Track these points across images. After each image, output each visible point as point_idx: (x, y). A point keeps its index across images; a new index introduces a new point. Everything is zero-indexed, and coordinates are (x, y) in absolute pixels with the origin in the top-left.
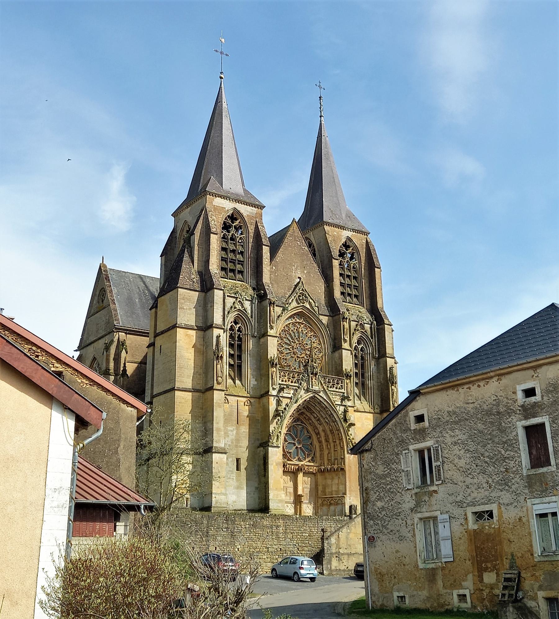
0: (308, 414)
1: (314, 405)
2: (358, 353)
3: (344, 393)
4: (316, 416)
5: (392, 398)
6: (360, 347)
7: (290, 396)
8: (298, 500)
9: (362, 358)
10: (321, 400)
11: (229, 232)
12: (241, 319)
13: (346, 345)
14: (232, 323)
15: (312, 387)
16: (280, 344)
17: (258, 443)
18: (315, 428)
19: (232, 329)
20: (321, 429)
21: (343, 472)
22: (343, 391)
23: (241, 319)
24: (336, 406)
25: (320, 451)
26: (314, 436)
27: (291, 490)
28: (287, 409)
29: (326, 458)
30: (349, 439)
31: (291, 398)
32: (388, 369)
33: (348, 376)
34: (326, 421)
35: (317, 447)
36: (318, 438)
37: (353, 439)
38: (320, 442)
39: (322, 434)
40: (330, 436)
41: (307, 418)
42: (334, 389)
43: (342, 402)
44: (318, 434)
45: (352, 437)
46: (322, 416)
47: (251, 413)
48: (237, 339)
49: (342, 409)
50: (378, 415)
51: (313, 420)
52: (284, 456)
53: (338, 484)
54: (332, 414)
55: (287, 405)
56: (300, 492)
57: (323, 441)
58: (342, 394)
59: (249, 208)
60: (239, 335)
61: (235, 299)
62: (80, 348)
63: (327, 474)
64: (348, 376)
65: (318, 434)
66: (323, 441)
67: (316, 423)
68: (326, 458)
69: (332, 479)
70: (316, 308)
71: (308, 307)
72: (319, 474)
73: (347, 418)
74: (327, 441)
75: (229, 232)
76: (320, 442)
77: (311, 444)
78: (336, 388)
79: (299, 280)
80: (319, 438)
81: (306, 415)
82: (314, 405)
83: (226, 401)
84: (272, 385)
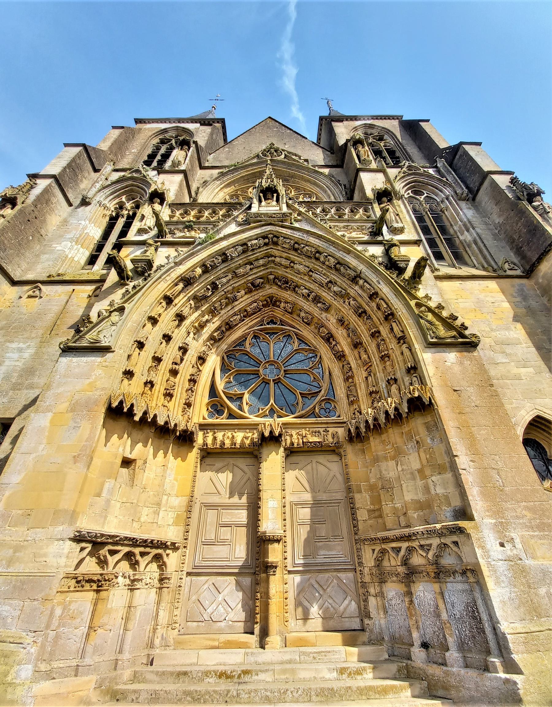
0: (287, 295)
10: (297, 235)
20: (331, 321)
21: (429, 419)
25: (346, 379)
26: (324, 350)
38: (340, 356)
39: (340, 334)
44: (329, 338)
57: (347, 350)
65: (329, 338)
66: (347, 350)
67: (315, 310)
76: (340, 356)
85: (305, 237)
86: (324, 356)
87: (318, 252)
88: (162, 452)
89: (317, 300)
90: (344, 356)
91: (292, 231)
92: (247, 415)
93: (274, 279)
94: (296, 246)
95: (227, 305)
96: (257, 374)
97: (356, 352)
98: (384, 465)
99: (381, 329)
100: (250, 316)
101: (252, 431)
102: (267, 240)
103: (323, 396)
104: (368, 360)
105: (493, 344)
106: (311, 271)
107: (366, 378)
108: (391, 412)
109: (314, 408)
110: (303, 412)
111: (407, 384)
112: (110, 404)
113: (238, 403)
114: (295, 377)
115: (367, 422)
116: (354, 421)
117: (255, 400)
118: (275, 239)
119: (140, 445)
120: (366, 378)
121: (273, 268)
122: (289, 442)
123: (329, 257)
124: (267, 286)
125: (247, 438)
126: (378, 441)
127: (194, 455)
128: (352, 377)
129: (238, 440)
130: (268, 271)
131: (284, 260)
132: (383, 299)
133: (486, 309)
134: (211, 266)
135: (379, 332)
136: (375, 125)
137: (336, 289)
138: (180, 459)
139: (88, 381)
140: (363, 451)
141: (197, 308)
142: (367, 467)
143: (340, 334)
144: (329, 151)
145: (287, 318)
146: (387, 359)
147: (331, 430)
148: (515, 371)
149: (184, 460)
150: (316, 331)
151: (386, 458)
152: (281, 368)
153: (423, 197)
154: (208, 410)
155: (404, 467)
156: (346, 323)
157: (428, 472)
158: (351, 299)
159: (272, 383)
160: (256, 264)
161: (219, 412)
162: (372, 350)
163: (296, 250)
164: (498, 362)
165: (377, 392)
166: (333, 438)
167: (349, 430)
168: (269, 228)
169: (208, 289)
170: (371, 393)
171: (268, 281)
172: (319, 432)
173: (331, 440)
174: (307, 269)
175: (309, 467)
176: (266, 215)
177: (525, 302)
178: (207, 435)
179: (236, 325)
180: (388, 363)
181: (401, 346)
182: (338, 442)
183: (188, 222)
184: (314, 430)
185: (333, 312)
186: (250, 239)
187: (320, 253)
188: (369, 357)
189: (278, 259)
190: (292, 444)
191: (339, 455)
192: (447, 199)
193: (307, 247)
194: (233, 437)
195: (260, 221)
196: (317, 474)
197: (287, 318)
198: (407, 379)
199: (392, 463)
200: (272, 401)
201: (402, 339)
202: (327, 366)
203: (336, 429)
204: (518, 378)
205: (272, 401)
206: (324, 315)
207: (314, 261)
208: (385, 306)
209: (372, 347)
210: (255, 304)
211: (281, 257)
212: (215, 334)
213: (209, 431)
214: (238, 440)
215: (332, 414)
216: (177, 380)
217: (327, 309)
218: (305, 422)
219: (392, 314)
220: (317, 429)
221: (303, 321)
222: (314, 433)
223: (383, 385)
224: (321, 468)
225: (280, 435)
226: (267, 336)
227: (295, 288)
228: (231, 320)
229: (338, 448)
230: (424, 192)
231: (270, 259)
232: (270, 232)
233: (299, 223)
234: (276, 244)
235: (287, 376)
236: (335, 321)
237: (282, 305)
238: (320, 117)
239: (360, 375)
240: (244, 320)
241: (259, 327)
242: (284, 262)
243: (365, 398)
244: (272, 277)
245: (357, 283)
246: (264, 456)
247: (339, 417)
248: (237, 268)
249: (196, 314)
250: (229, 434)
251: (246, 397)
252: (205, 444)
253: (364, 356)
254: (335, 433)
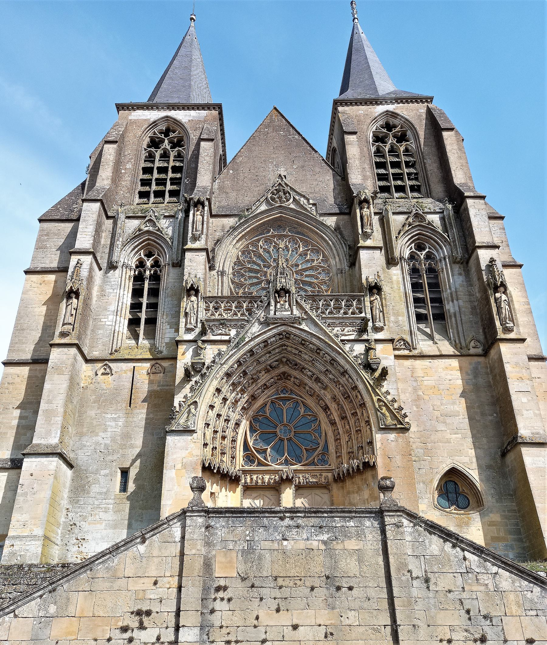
1: (297, 352)
2: (420, 264)
4: (309, 373)
5: (499, 312)
7: (226, 338)
9: (431, 270)
10: (304, 335)
12: (156, 248)
15: (275, 314)
16: (238, 272)
18: (319, 398)
20: (327, 397)
22: (363, 315)
23: (156, 248)
24: (341, 345)
25: (336, 440)
26: (322, 416)
30: (379, 400)
31: (229, 341)
34: (330, 379)
35: (330, 434)
36: (328, 416)
37: (394, 401)
39: (333, 406)
41: (297, 382)
44: (326, 408)
45: (390, 398)
47: (163, 385)
50: (481, 359)
57: (337, 420)
59: (193, 113)
65: (326, 408)
66: (337, 420)
67: (316, 387)
70: (311, 206)
73: (371, 361)
76: (333, 423)
80: (330, 415)
81: (295, 378)
82: (297, 352)
83: (108, 370)
84: (186, 325)
85: (309, 338)
86: (322, 421)
87: (319, 349)
88: (224, 488)
89: (318, 380)
90: (335, 423)
91: (300, 332)
92: (270, 464)
93: (286, 361)
94: (303, 342)
95: (252, 383)
96: (275, 433)
97: (343, 422)
98: (352, 496)
99: (358, 411)
100: (268, 388)
101: (274, 474)
102: (281, 336)
103: (320, 451)
104: (349, 429)
105: (439, 416)
106: (313, 360)
107: (347, 442)
108: (355, 468)
109: (314, 459)
110: (307, 462)
111: (367, 451)
112: (204, 465)
113: (264, 455)
114: (302, 436)
115: (343, 472)
116: (337, 470)
117: (274, 453)
118: (288, 335)
119: (215, 484)
120: (347, 442)
121: (285, 353)
122: (297, 481)
123: (326, 355)
124: (281, 366)
125: (272, 479)
126: (350, 482)
127: (239, 489)
128: (340, 439)
129: (266, 480)
130: (282, 355)
131: (294, 350)
132: (359, 392)
133: (443, 385)
134: (243, 362)
135: (356, 413)
136: (398, 115)
137: (330, 376)
138: (232, 492)
139: (187, 452)
140: (343, 488)
141: (234, 390)
142: (344, 497)
143: (333, 407)
144: (340, 176)
145: (296, 389)
146: (359, 432)
147: (324, 474)
148: (449, 436)
149: (234, 492)
150: (317, 401)
151: (353, 492)
152: (292, 429)
153: (424, 253)
154: (243, 460)
155: (361, 498)
156: (337, 400)
157: (369, 500)
158: (341, 386)
159: (286, 441)
160: (273, 352)
161: (252, 462)
162: (352, 424)
163: (303, 345)
164: (439, 430)
165: (352, 452)
166: (325, 480)
167: (334, 476)
168: (283, 328)
169: (241, 377)
170: (349, 453)
171: (282, 362)
172: (316, 475)
173: (323, 481)
174: (310, 358)
175: (310, 496)
176: (281, 319)
177: (475, 379)
178: (247, 477)
179: (259, 396)
180: (359, 435)
181: (367, 426)
182: (328, 482)
183: (222, 320)
184: (313, 474)
185: (329, 390)
186: (269, 338)
187: (321, 350)
188: (350, 428)
189: (289, 349)
190: (299, 483)
191: (329, 489)
192: (445, 259)
193: (311, 345)
194: (263, 478)
195: (277, 323)
196: (315, 500)
197: (296, 389)
198: (367, 448)
199: (356, 495)
200: (286, 454)
202: (324, 429)
203: (327, 474)
204: (448, 441)
205: (286, 454)
206: (323, 391)
207: (316, 354)
208: (360, 398)
209: (352, 421)
210: (272, 380)
211: (292, 347)
212: (245, 406)
213: (247, 474)
214: (266, 480)
215: (326, 462)
216: (226, 442)
217: (325, 388)
218: (308, 469)
219: (364, 404)
220: (315, 474)
221: (307, 392)
222: (313, 476)
223: (355, 448)
224: (317, 498)
225: (292, 478)
226: (281, 403)
227: (302, 369)
228: (256, 393)
229: (328, 485)
230: (427, 245)
231: (284, 347)
232: (284, 331)
233: (305, 321)
234: (288, 338)
235: (297, 435)
236: (330, 397)
237: (292, 379)
238: (334, 101)
239: (344, 438)
240: (264, 392)
241: (275, 397)
242: (294, 351)
243: (346, 455)
244: (284, 360)
245: (344, 376)
246: (282, 490)
247: (330, 465)
248: (260, 358)
249: (233, 395)
250: (260, 476)
251: (269, 450)
252: (246, 482)
253: (347, 427)
254: (326, 476)
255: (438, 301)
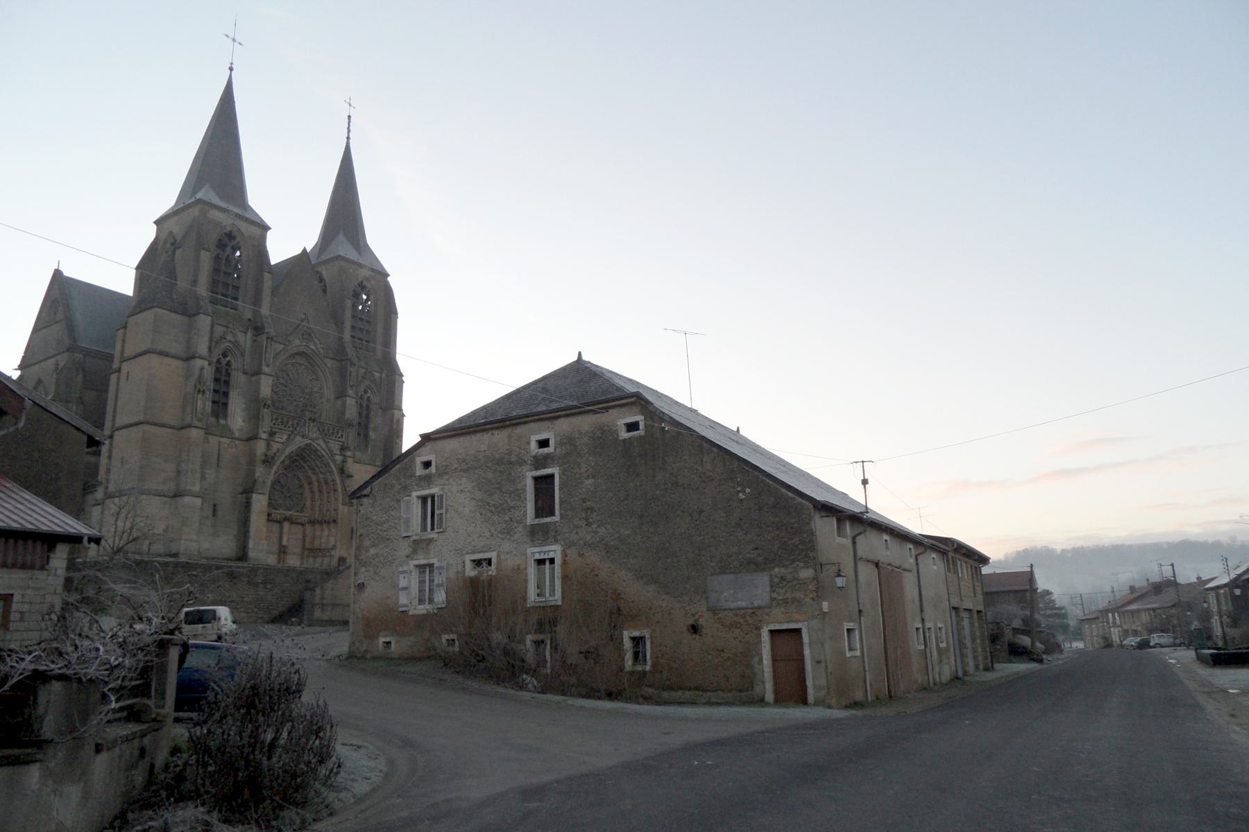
3: (343, 442)
6: (366, 396)
7: (282, 441)
8: (283, 551)
10: (318, 448)
11: (224, 251)
13: (351, 392)
14: (219, 355)
17: (240, 489)
19: (219, 361)
22: (344, 440)
23: (230, 351)
26: (306, 486)
27: (275, 540)
28: (278, 454)
29: (317, 509)
31: (283, 443)
32: (395, 422)
33: (350, 425)
36: (311, 488)
39: (316, 484)
40: (324, 487)
42: (334, 438)
43: (340, 452)
44: (310, 483)
46: (317, 466)
48: (224, 373)
49: (339, 458)
51: (307, 468)
52: (270, 505)
53: (328, 535)
54: (328, 463)
55: (278, 450)
56: (284, 542)
58: (341, 443)
60: (227, 370)
61: (225, 329)
62: (21, 367)
63: (317, 527)
64: (350, 425)
68: (317, 509)
69: (322, 530)
71: (313, 347)
72: (307, 525)
74: (320, 491)
75: (224, 251)
77: (302, 494)
78: (336, 437)
79: (304, 316)
168: (310, 441)
201: (336, 499)
255: (366, 427)
